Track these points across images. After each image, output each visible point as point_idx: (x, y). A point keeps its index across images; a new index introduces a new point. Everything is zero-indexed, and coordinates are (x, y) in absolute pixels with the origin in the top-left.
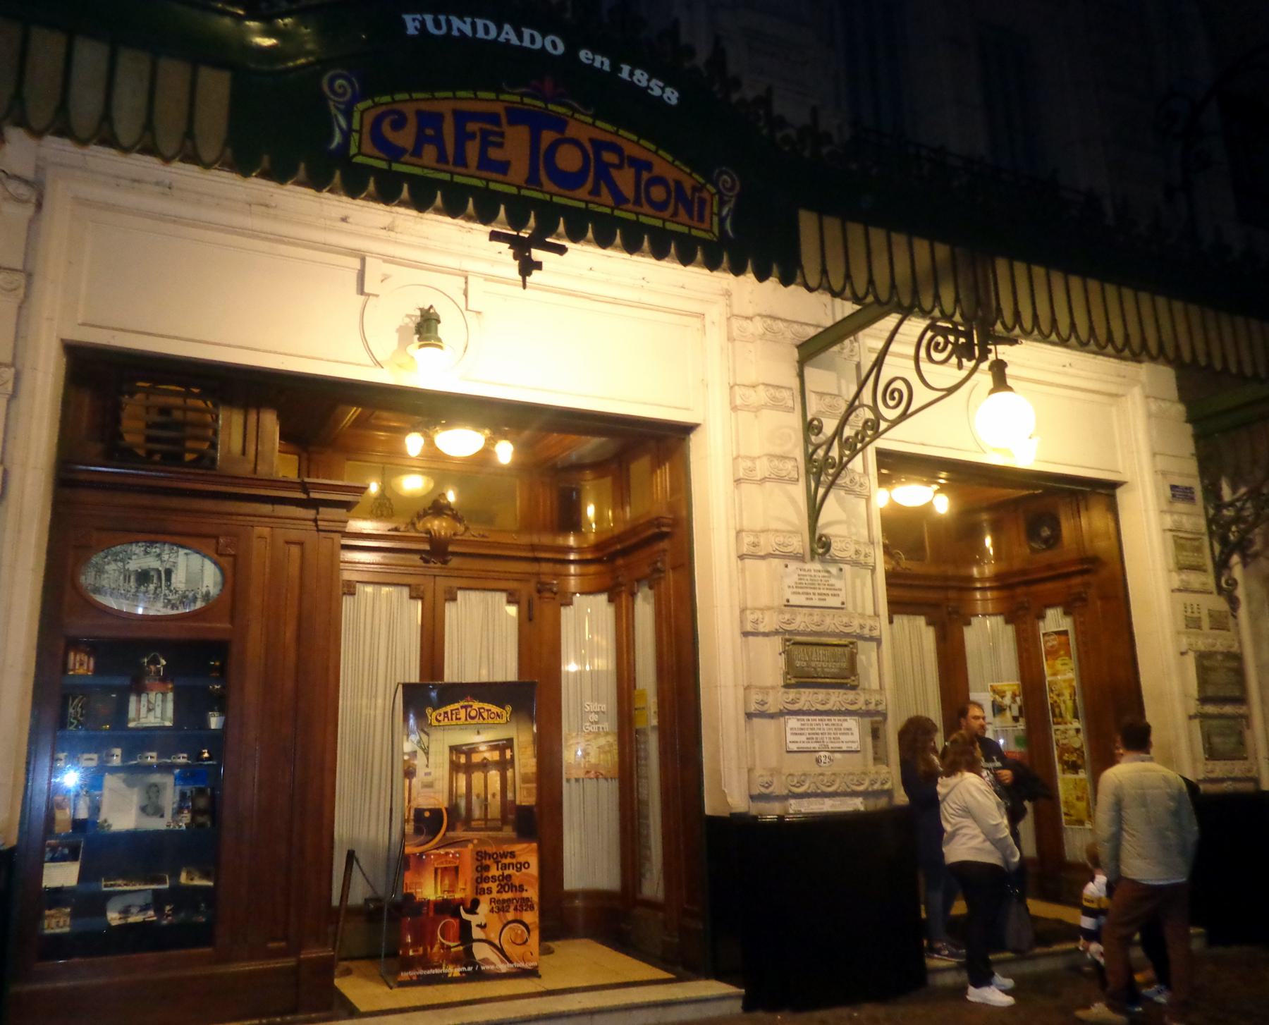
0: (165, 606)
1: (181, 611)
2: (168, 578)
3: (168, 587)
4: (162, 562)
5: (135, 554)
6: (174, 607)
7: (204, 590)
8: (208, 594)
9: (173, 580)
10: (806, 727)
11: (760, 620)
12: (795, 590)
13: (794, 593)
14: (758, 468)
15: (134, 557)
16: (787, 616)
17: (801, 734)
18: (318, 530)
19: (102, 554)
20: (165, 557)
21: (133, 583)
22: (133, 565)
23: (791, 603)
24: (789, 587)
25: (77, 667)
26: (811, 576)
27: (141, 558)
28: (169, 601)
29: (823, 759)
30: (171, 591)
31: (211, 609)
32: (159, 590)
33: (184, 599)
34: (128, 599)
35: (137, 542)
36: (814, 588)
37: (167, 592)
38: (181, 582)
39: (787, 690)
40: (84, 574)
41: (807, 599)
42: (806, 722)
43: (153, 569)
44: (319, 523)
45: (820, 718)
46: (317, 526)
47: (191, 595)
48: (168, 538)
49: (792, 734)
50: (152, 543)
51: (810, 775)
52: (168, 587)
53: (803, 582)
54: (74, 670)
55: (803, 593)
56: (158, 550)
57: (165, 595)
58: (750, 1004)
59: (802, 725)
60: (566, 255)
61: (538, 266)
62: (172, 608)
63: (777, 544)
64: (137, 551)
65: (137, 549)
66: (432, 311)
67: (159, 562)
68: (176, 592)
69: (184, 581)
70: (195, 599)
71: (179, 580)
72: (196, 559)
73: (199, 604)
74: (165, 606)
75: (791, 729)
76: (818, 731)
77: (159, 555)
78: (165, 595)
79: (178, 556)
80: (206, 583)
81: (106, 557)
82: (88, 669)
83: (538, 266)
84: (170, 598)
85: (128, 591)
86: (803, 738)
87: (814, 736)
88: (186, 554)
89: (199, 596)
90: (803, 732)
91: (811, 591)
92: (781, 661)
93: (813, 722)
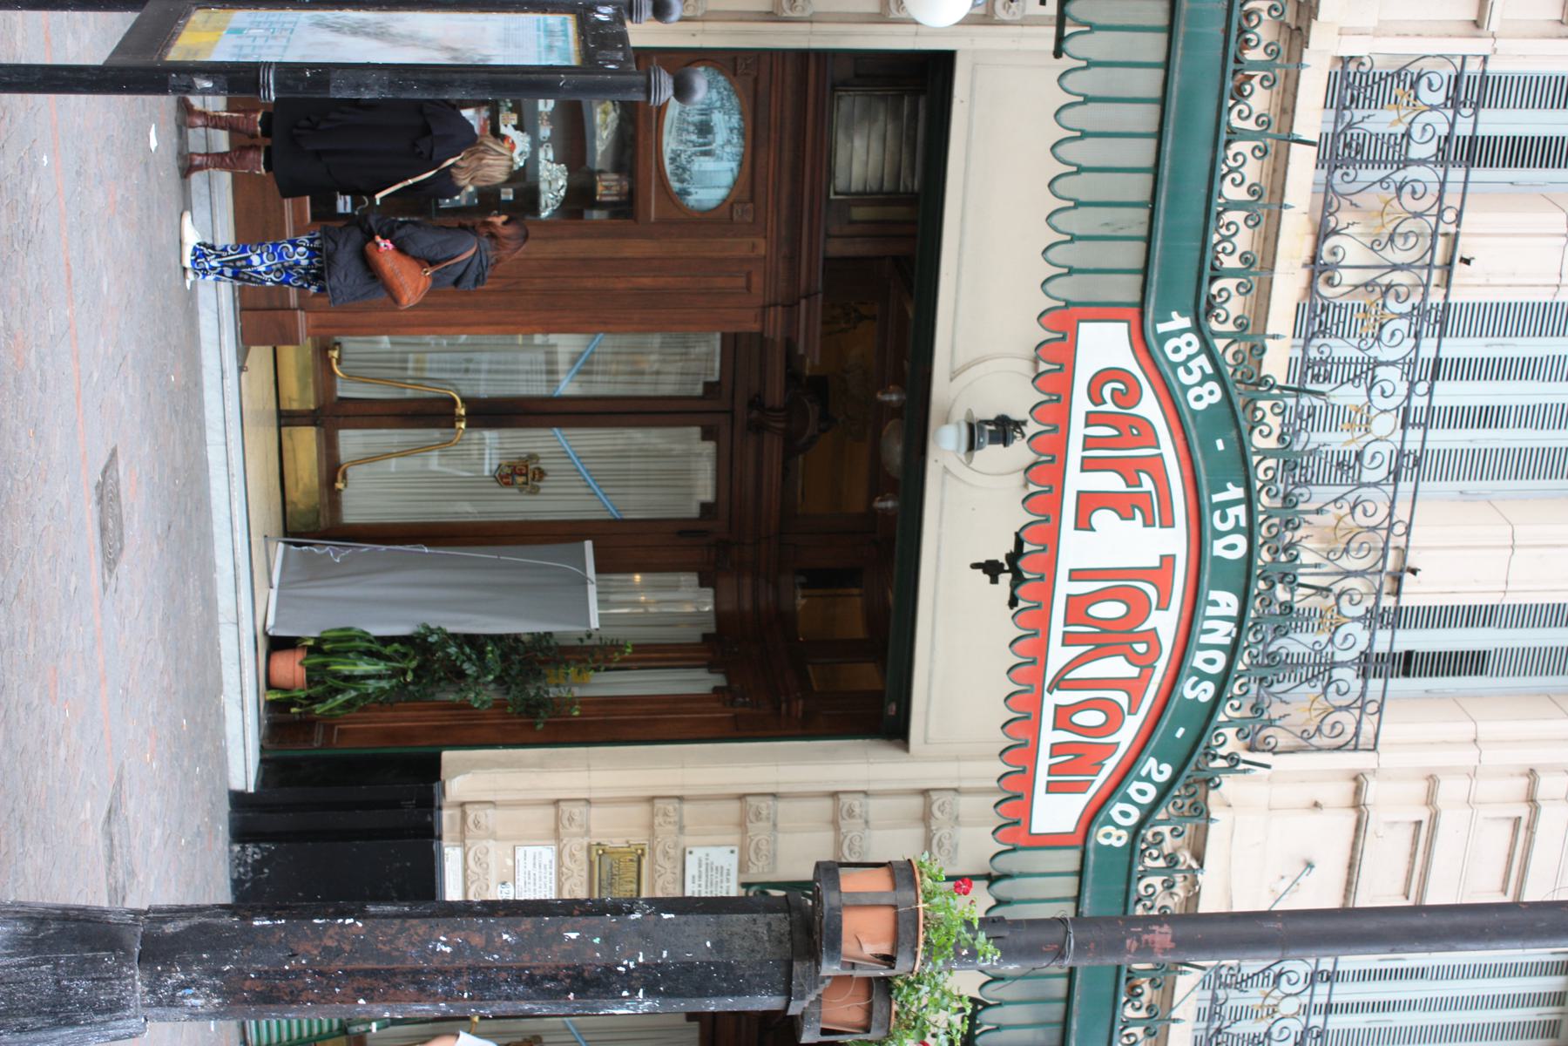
0: (673, 151)
1: (668, 168)
2: (705, 154)
3: (695, 154)
4: (723, 146)
5: (730, 118)
6: (673, 160)
7: (692, 190)
8: (689, 194)
9: (702, 158)
10: (543, 871)
11: (668, 819)
12: (704, 862)
13: (700, 860)
14: (854, 821)
15: (727, 117)
16: (672, 852)
17: (534, 864)
18: (764, 307)
19: (728, 86)
20: (728, 149)
21: (697, 118)
22: (718, 119)
23: (688, 857)
24: (707, 855)
25: (604, 183)
26: (722, 882)
27: (726, 124)
28: (679, 156)
29: (505, 890)
30: (690, 157)
31: (674, 199)
32: (691, 145)
33: (681, 171)
34: (680, 114)
35: (742, 119)
36: (707, 886)
37: (689, 153)
38: (700, 166)
39: (585, 848)
40: (706, 70)
41: (694, 877)
42: (548, 870)
43: (714, 138)
44: (772, 309)
45: (554, 888)
46: (770, 306)
47: (686, 176)
48: (749, 150)
49: (535, 854)
50: (743, 135)
51: (487, 873)
52: (695, 154)
53: (714, 873)
54: (601, 180)
55: (700, 871)
56: (735, 141)
57: (685, 151)
58: (238, 800)
59: (545, 866)
60: (1008, 607)
61: (994, 581)
62: (671, 159)
63: (759, 841)
64: (733, 120)
65: (735, 120)
66: (1019, 435)
67: (721, 143)
68: (689, 162)
69: (702, 169)
70: (682, 181)
71: (703, 165)
72: (727, 179)
73: (675, 185)
74: (673, 151)
75: (540, 853)
76: (538, 885)
77: (729, 142)
78: (685, 151)
79: (729, 161)
80: (700, 191)
81: (725, 89)
82: (602, 195)
83: (994, 581)
84: (683, 156)
85: (688, 114)
86: (530, 867)
87: (532, 881)
88: (732, 170)
89: (685, 185)
90: (537, 866)
91: (703, 883)
92: (618, 842)
93: (548, 880)
